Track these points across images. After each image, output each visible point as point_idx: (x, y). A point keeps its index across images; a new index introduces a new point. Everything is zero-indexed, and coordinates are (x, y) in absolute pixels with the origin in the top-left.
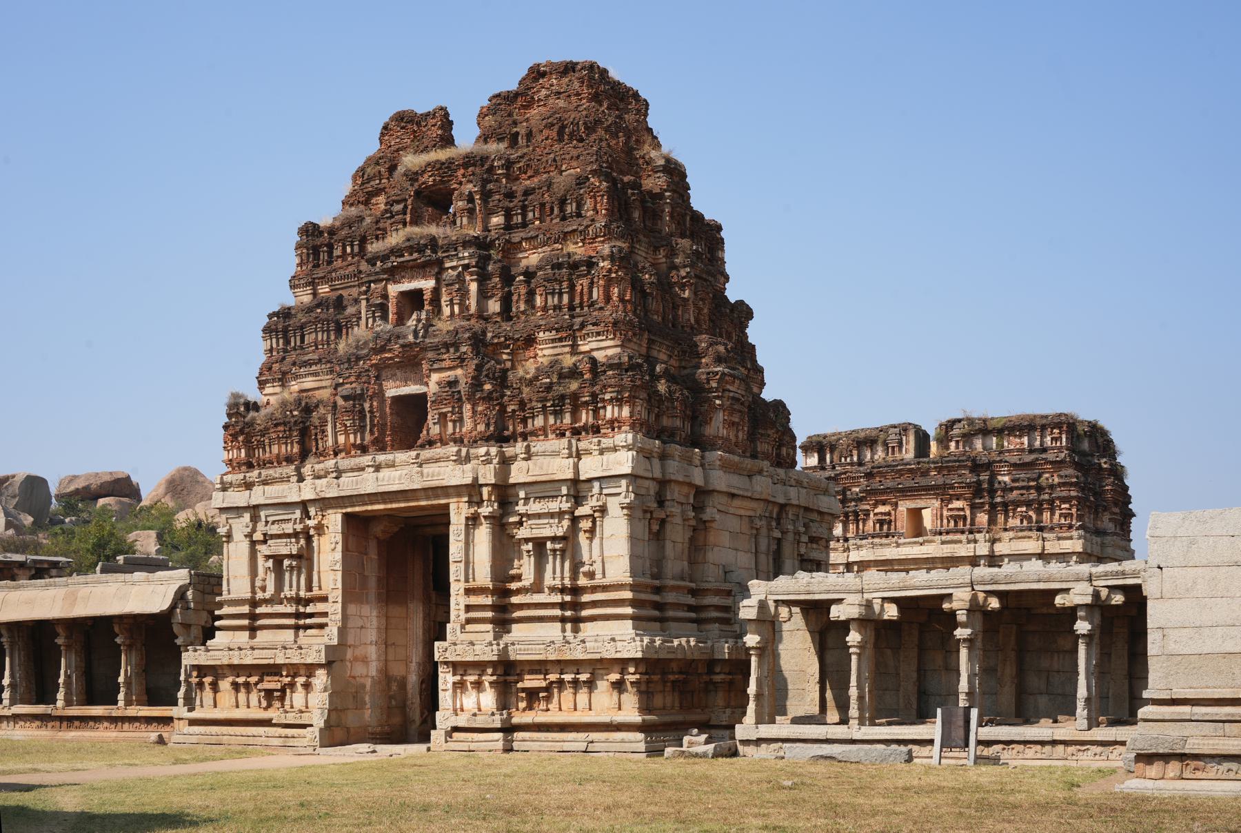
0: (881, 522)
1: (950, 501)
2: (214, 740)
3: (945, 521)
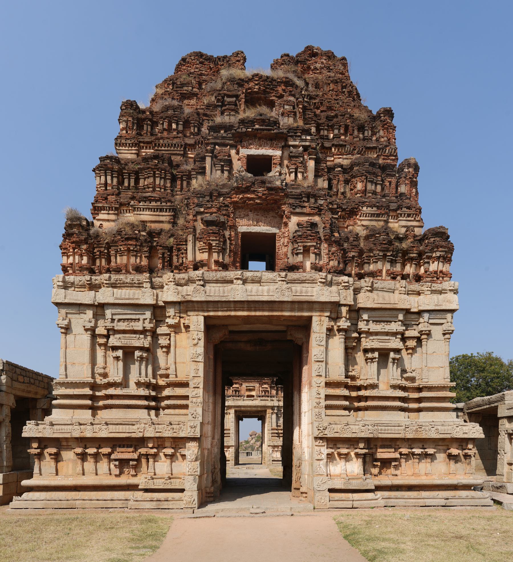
0: (236, 391)
1: (262, 384)
2: (64, 504)
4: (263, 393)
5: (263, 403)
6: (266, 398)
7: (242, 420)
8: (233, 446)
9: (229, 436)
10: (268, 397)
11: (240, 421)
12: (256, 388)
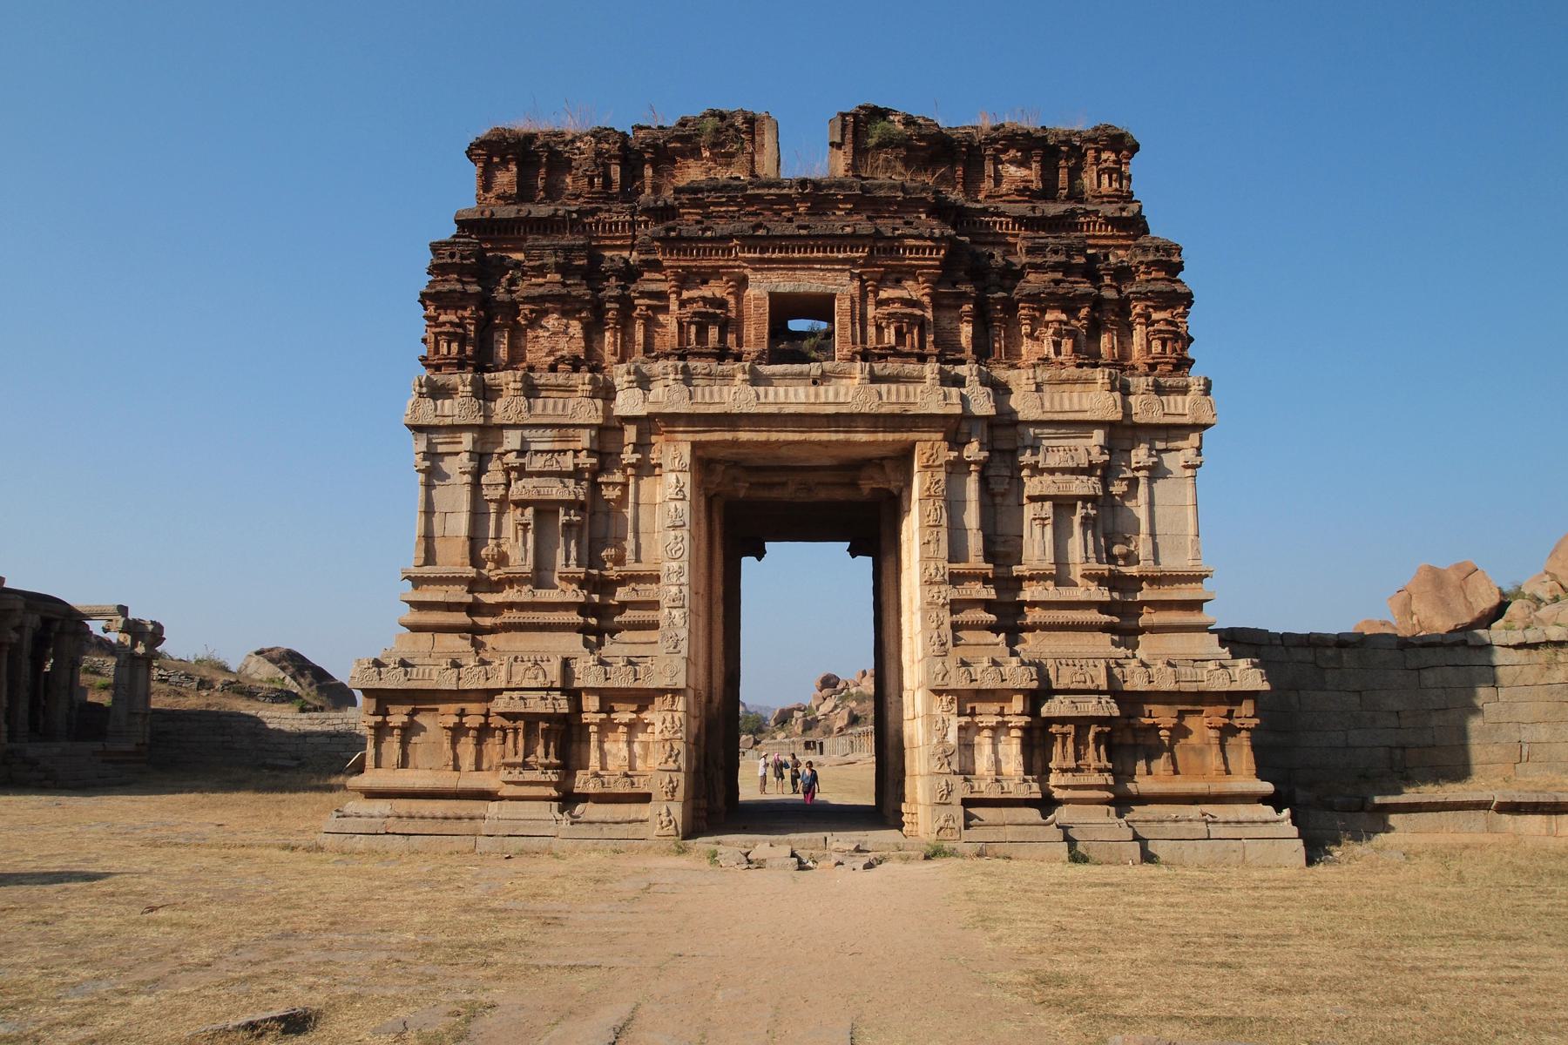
1: (881, 282)
3: (872, 331)
4: (890, 337)
5: (890, 399)
6: (911, 368)
7: (760, 554)
8: (675, 692)
9: (654, 626)
10: (922, 359)
11: (748, 562)
12: (841, 307)
